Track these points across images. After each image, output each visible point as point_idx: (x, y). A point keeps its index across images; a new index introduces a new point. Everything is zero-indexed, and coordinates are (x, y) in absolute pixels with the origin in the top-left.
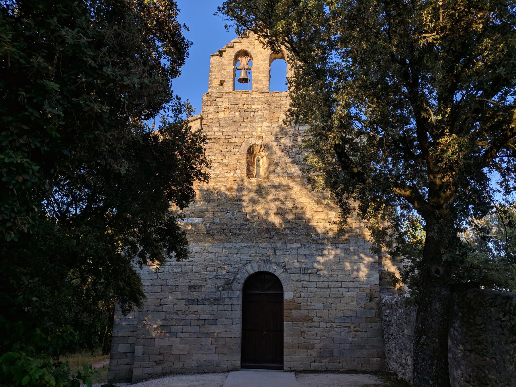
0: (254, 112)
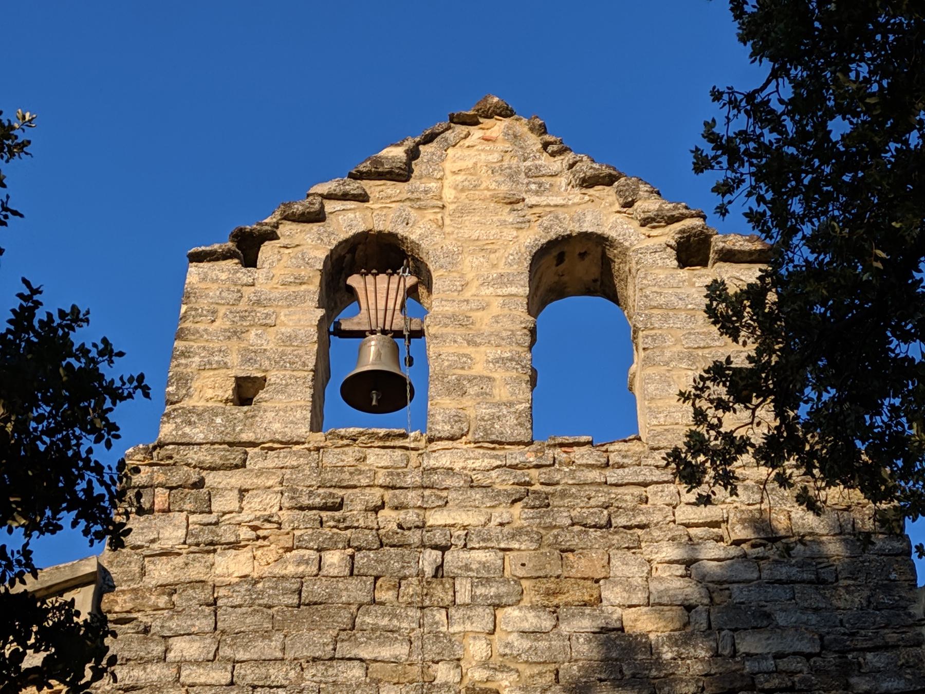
0: (444, 549)
